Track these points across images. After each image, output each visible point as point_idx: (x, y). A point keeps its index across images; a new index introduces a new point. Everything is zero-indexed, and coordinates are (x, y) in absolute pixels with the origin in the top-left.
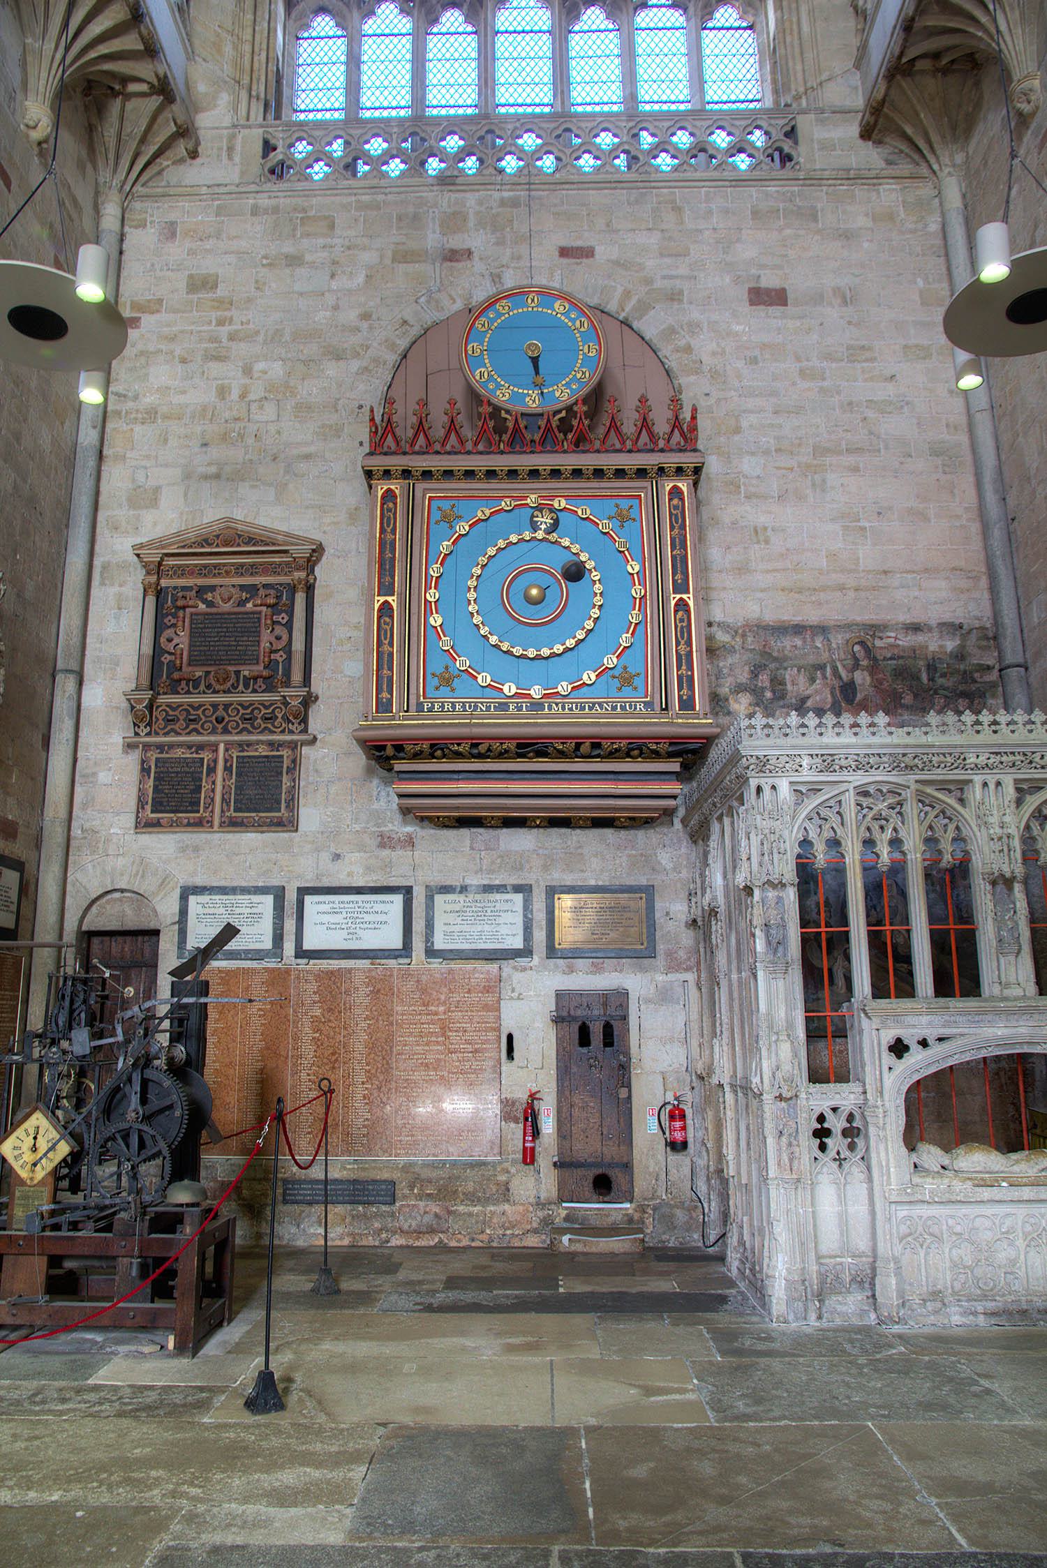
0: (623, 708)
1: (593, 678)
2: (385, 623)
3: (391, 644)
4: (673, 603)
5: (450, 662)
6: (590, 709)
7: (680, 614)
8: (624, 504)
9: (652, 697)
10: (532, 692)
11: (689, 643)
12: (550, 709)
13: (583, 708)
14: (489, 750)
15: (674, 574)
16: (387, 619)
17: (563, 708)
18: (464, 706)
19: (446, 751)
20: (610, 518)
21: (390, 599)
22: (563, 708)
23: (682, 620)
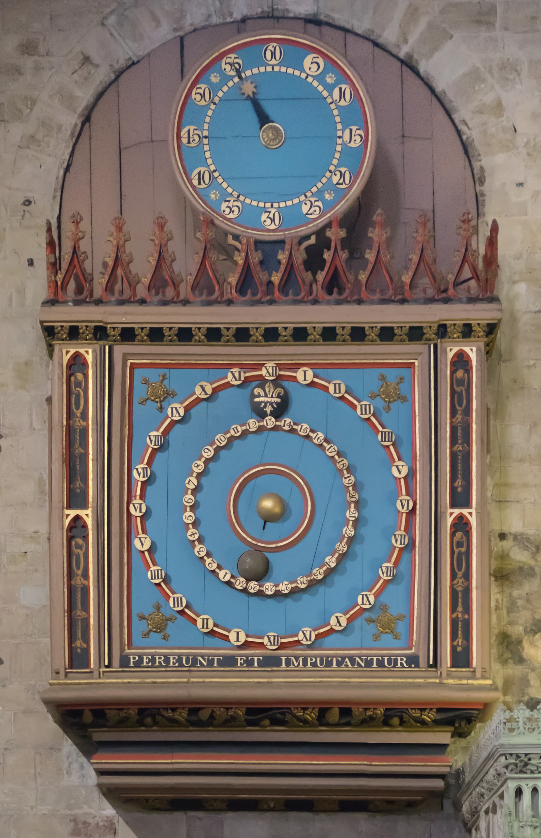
0: (380, 664)
1: (344, 623)
2: (78, 547)
3: (86, 576)
4: (450, 520)
5: (162, 601)
6: (339, 664)
7: (459, 534)
8: (392, 375)
9: (418, 649)
10: (265, 641)
11: (467, 576)
12: (288, 663)
13: (329, 664)
14: (212, 716)
15: (453, 479)
16: (80, 541)
17: (305, 664)
18: (180, 660)
19: (159, 718)
20: (373, 397)
21: (82, 513)
22: (305, 664)
23: (460, 544)
